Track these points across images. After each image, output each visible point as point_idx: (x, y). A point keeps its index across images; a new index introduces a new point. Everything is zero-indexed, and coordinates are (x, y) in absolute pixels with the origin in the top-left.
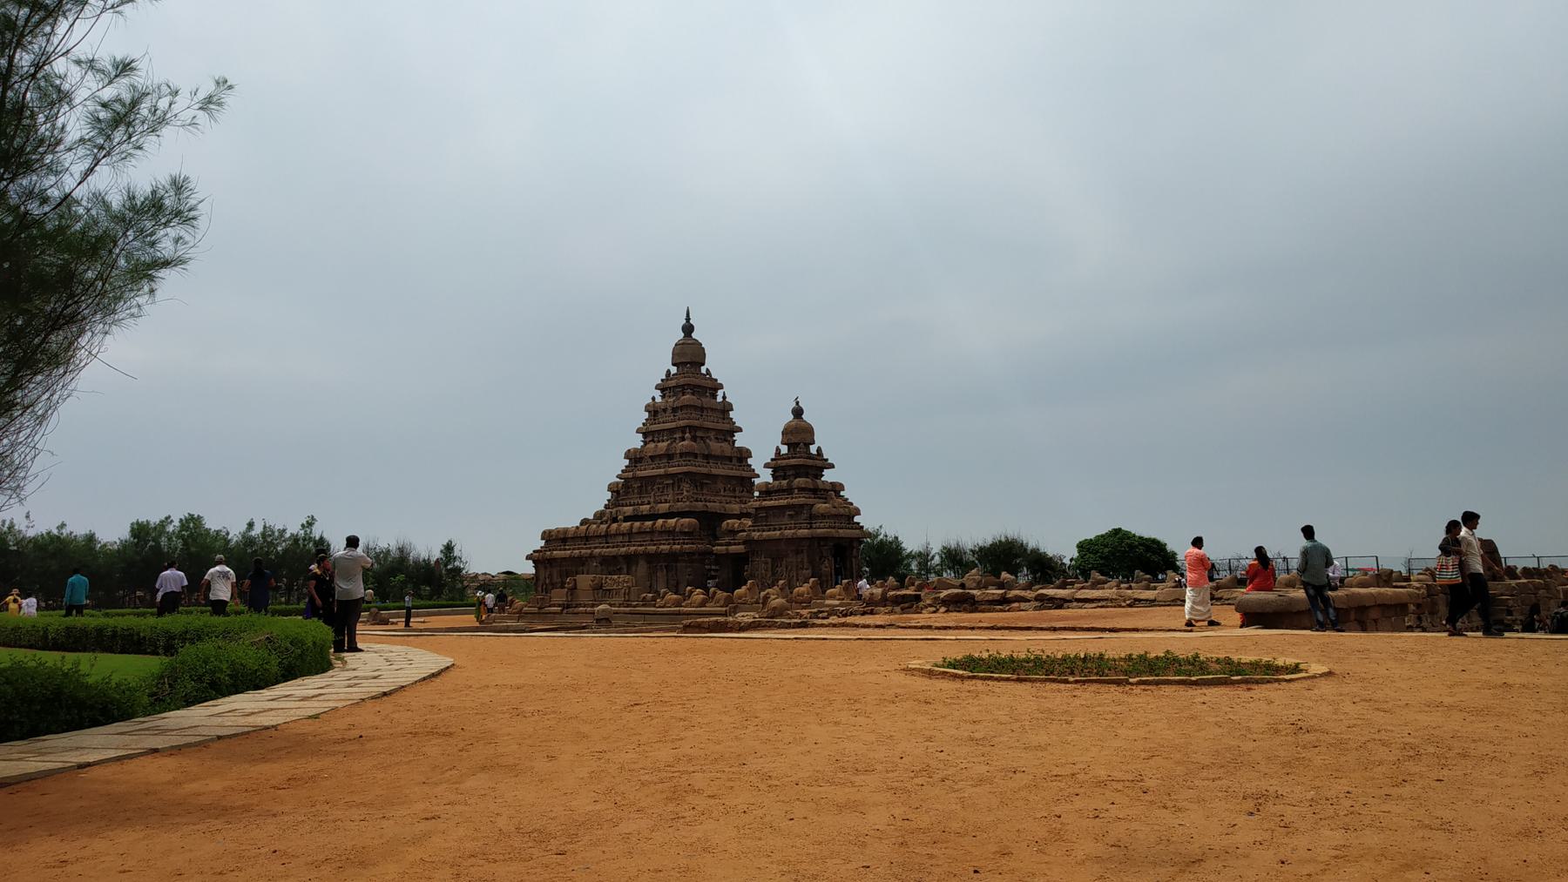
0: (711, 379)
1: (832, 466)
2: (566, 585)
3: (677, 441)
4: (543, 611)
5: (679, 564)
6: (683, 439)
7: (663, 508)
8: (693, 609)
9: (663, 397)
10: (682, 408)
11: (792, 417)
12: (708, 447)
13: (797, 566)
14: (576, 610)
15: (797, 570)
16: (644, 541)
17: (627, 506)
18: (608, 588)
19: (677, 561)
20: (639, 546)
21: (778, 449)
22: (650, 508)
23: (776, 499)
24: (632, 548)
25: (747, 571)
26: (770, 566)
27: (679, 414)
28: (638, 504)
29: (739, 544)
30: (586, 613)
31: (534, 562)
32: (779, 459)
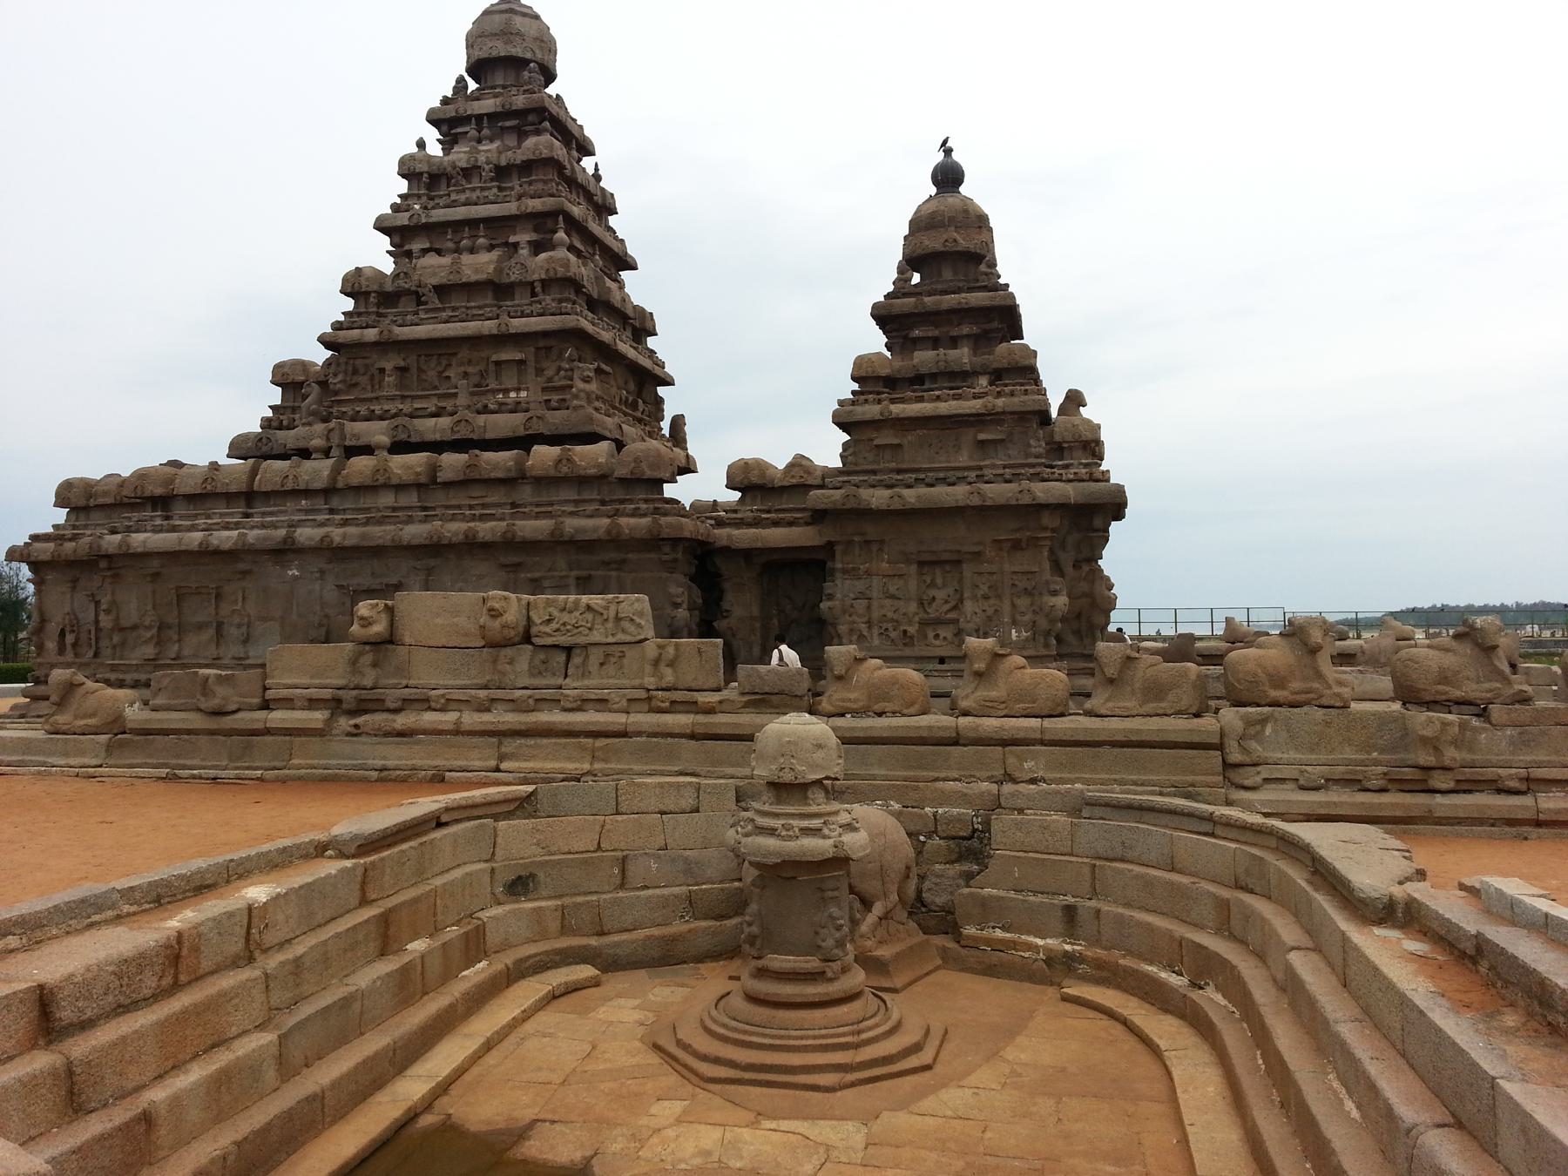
0: (575, 120)
2: (355, 628)
3: (524, 252)
4: (227, 722)
6: (537, 248)
7: (503, 424)
9: (448, 142)
10: (527, 167)
14: (402, 721)
16: (484, 506)
20: (473, 518)
21: (901, 271)
22: (460, 421)
23: (938, 398)
24: (463, 526)
25: (831, 597)
26: (913, 585)
27: (515, 183)
29: (791, 524)
30: (457, 732)
31: (35, 566)
32: (920, 294)
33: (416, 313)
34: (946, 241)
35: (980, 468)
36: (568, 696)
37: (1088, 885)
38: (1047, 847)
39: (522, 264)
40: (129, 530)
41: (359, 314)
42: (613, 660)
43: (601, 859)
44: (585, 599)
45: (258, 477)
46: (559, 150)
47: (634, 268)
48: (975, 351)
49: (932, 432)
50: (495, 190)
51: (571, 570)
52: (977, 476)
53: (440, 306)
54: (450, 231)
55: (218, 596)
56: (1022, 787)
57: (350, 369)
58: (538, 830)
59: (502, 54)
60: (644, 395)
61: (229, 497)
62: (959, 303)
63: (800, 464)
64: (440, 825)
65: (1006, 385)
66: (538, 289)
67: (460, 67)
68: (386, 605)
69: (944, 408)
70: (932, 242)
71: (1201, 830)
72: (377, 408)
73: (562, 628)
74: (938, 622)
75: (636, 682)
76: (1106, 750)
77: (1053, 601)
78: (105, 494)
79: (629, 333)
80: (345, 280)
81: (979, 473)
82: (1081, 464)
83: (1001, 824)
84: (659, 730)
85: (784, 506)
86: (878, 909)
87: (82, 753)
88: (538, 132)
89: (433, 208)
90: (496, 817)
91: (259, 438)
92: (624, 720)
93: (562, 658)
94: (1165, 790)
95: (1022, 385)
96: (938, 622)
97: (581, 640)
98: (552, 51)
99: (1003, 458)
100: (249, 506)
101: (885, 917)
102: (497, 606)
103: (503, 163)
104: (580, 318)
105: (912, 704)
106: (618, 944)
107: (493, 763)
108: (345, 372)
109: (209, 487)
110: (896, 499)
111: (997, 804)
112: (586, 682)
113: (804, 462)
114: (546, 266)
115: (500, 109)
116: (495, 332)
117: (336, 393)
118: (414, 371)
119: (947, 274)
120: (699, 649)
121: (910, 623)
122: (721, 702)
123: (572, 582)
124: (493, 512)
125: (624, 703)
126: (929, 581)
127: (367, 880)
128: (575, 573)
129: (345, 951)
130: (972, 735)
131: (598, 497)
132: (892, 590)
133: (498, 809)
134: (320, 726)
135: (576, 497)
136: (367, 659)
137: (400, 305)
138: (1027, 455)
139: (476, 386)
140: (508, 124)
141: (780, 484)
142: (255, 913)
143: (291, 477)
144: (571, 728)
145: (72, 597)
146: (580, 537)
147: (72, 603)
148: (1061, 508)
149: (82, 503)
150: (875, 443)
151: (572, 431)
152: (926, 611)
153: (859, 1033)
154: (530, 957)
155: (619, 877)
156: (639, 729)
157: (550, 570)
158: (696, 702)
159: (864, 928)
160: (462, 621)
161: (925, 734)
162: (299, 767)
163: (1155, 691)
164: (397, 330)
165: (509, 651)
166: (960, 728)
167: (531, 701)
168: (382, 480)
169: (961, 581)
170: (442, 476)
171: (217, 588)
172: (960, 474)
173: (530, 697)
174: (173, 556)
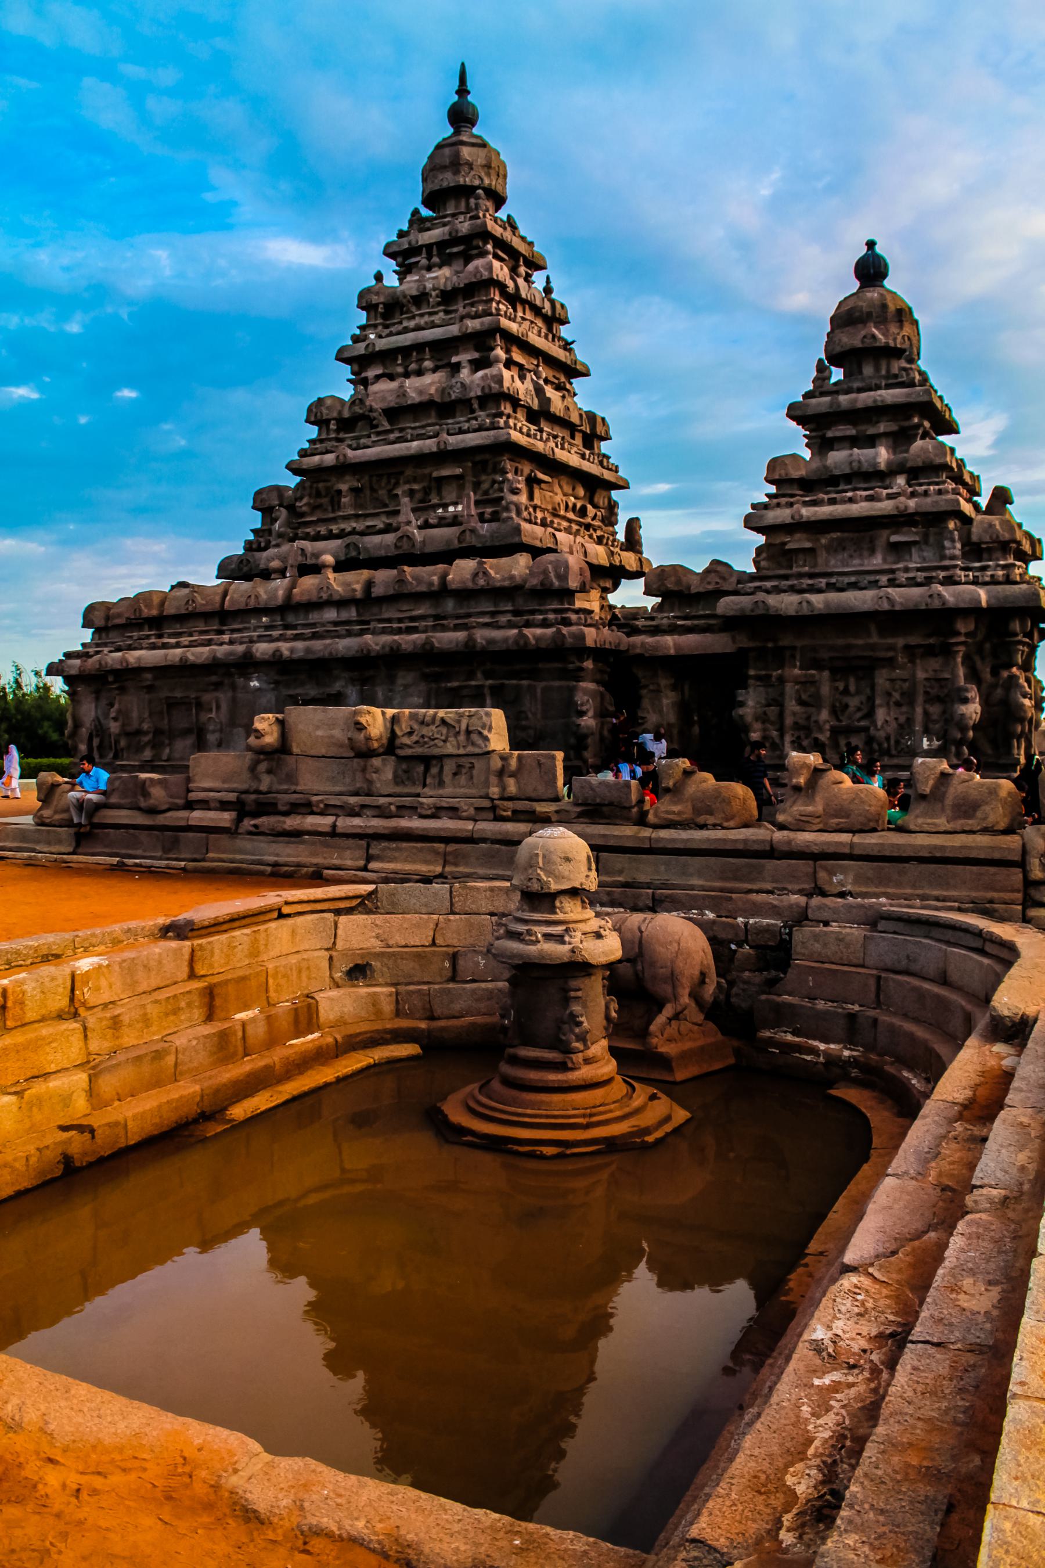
1: (951, 428)
5: (540, 685)
6: (477, 365)
8: (845, 837)
11: (857, 284)
12: (539, 391)
13: (926, 693)
15: (925, 702)
17: (318, 537)
18: (419, 750)
19: (533, 674)
20: (399, 631)
21: (821, 368)
22: (402, 537)
23: (851, 500)
25: (742, 704)
26: (825, 690)
27: (460, 308)
28: (350, 533)
31: (68, 680)
32: (837, 393)
33: (369, 436)
34: (865, 337)
35: (893, 571)
36: (422, 804)
37: (873, 996)
38: (841, 959)
39: (462, 383)
40: (130, 648)
41: (321, 441)
42: (464, 771)
43: (434, 953)
44: (441, 713)
45: (228, 598)
46: (501, 271)
47: (587, 374)
48: (894, 448)
49: (846, 535)
50: (441, 314)
51: (487, 678)
52: (889, 580)
53: (389, 428)
54: (400, 357)
55: (199, 705)
56: (828, 901)
57: (314, 492)
58: (377, 925)
59: (452, 185)
60: (596, 500)
61: (206, 616)
62: (875, 401)
63: (717, 568)
64: (281, 916)
65: (921, 485)
66: (476, 406)
67: (416, 202)
68: (277, 719)
69: (860, 509)
70: (852, 339)
71: (974, 945)
72: (335, 528)
73: (421, 740)
74: (849, 731)
75: (482, 793)
76: (912, 868)
77: (963, 709)
78: (119, 615)
79: (578, 440)
80: (309, 410)
81: (891, 576)
82: (998, 565)
83: (802, 935)
84: (499, 837)
85: (701, 613)
86: (668, 1011)
87: (60, 842)
88: (483, 254)
89: (388, 336)
90: (338, 912)
91: (241, 560)
92: (470, 827)
93: (421, 769)
94: (964, 906)
95: (937, 484)
96: (849, 731)
97: (436, 751)
98: (502, 174)
99: (918, 560)
100: (223, 623)
101: (676, 1016)
102: (363, 720)
103: (449, 288)
104: (512, 432)
105: (732, 818)
106: (443, 1029)
107: (362, 863)
108: (310, 496)
109: (190, 609)
110: (804, 604)
111: (802, 917)
112: (441, 792)
113: (720, 568)
114: (482, 384)
115: (447, 237)
116: (435, 449)
117: (303, 515)
118: (368, 492)
119: (868, 370)
120: (539, 761)
121: (820, 729)
122: (557, 812)
123: (486, 691)
124: (416, 624)
125: (472, 811)
126: (841, 688)
127: (195, 958)
128: (490, 682)
129: (167, 1015)
130: (786, 848)
131: (510, 608)
132: (804, 697)
133: (342, 905)
134: (227, 825)
135: (492, 609)
136: (263, 767)
137: (358, 428)
138: (943, 557)
139: (421, 501)
140: (455, 250)
141: (696, 591)
142: (77, 978)
143: (253, 597)
144: (425, 833)
145: (96, 707)
146: (491, 648)
147: (96, 712)
148: (974, 611)
149: (101, 623)
150: (787, 547)
151: (502, 543)
152: (841, 721)
153: (591, 1115)
154: (360, 1034)
155: (450, 970)
156: (484, 836)
157: (466, 680)
158: (534, 812)
159: (653, 1028)
160: (337, 733)
161: (741, 847)
162: (213, 860)
163: (967, 808)
164: (350, 453)
165: (376, 762)
166: (774, 842)
167: (393, 808)
168: (325, 596)
169: (873, 688)
170: (377, 591)
171: (197, 698)
172: (872, 578)
173: (391, 804)
174: (162, 671)
